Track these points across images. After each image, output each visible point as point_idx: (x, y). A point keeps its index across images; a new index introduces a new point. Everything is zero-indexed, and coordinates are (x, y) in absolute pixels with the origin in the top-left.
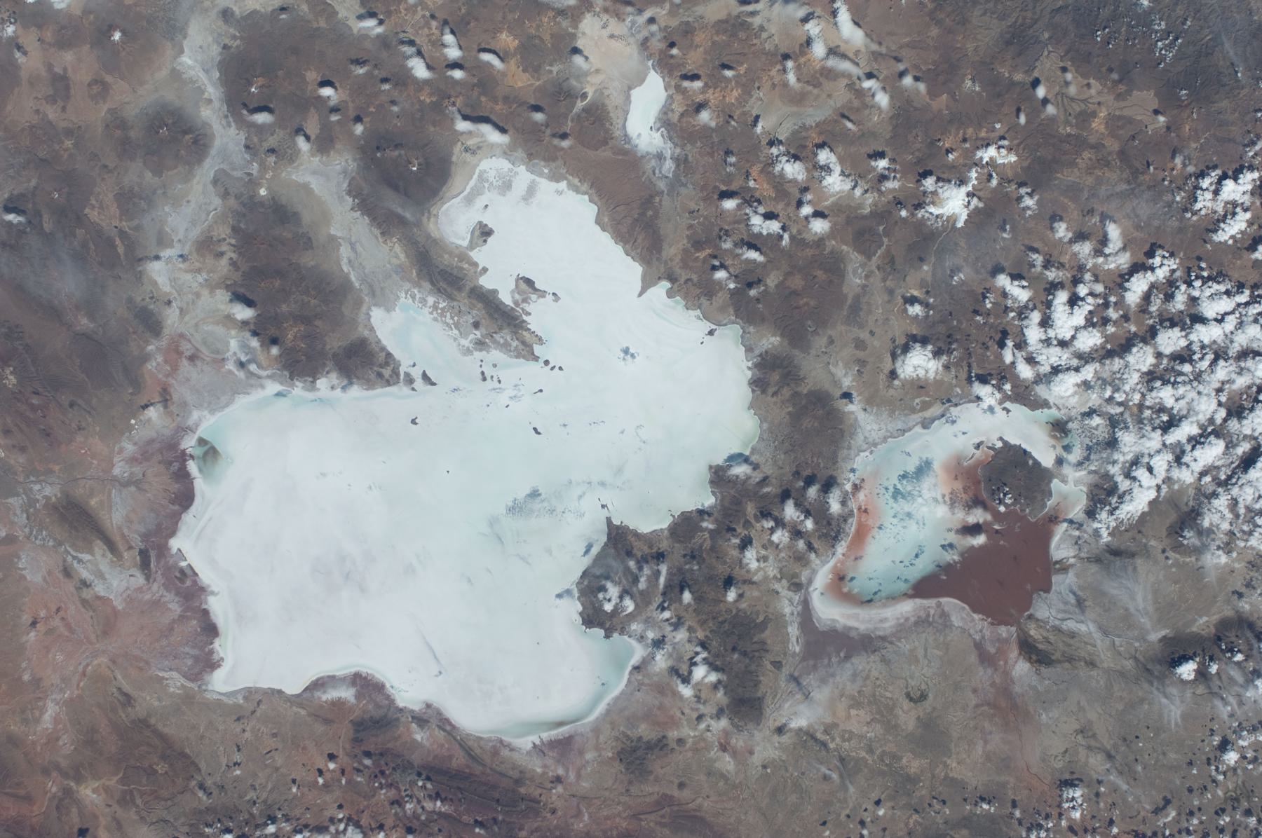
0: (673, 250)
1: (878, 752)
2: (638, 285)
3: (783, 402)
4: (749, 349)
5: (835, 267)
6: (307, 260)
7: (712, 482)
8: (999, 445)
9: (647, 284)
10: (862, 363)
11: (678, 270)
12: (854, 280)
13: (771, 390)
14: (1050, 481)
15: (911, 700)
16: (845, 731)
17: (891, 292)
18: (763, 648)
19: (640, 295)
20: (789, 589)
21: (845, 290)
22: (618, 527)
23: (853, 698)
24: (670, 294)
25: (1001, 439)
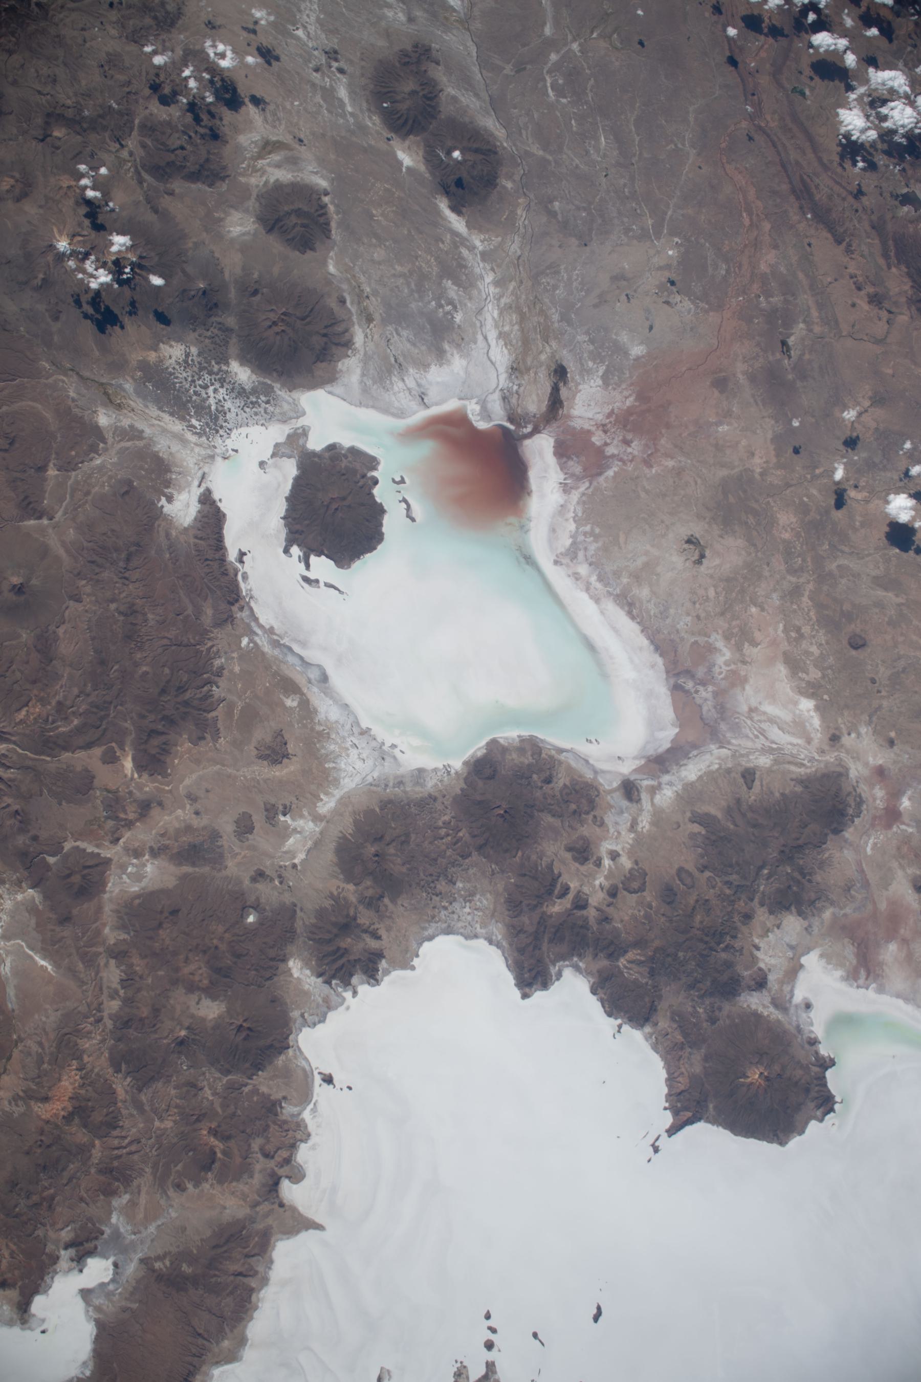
0: (229, 1202)
1: (794, 579)
2: (307, 1237)
3: (381, 918)
4: (329, 1006)
5: (145, 913)
7: (545, 986)
8: (295, 550)
9: (301, 1223)
10: (271, 812)
11: (257, 1179)
12: (152, 874)
13: (373, 944)
14: (314, 454)
15: (702, 556)
16: (788, 639)
17: (145, 808)
18: (736, 808)
19: (319, 1227)
20: (639, 801)
21: (170, 882)
22: (676, 1112)
23: (739, 648)
24: (297, 1176)
25: (286, 551)
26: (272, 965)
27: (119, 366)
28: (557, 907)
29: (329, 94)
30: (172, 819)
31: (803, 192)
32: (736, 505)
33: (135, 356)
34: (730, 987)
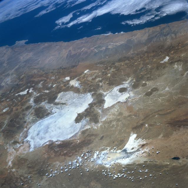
0: (81, 91)
5: (99, 85)
6: (42, 109)
26: (94, 91)
27: (134, 78)
28: (93, 105)
29: (154, 86)
30: (104, 85)
31: (147, 117)
32: (120, 114)
33: (134, 79)
34: (85, 116)
